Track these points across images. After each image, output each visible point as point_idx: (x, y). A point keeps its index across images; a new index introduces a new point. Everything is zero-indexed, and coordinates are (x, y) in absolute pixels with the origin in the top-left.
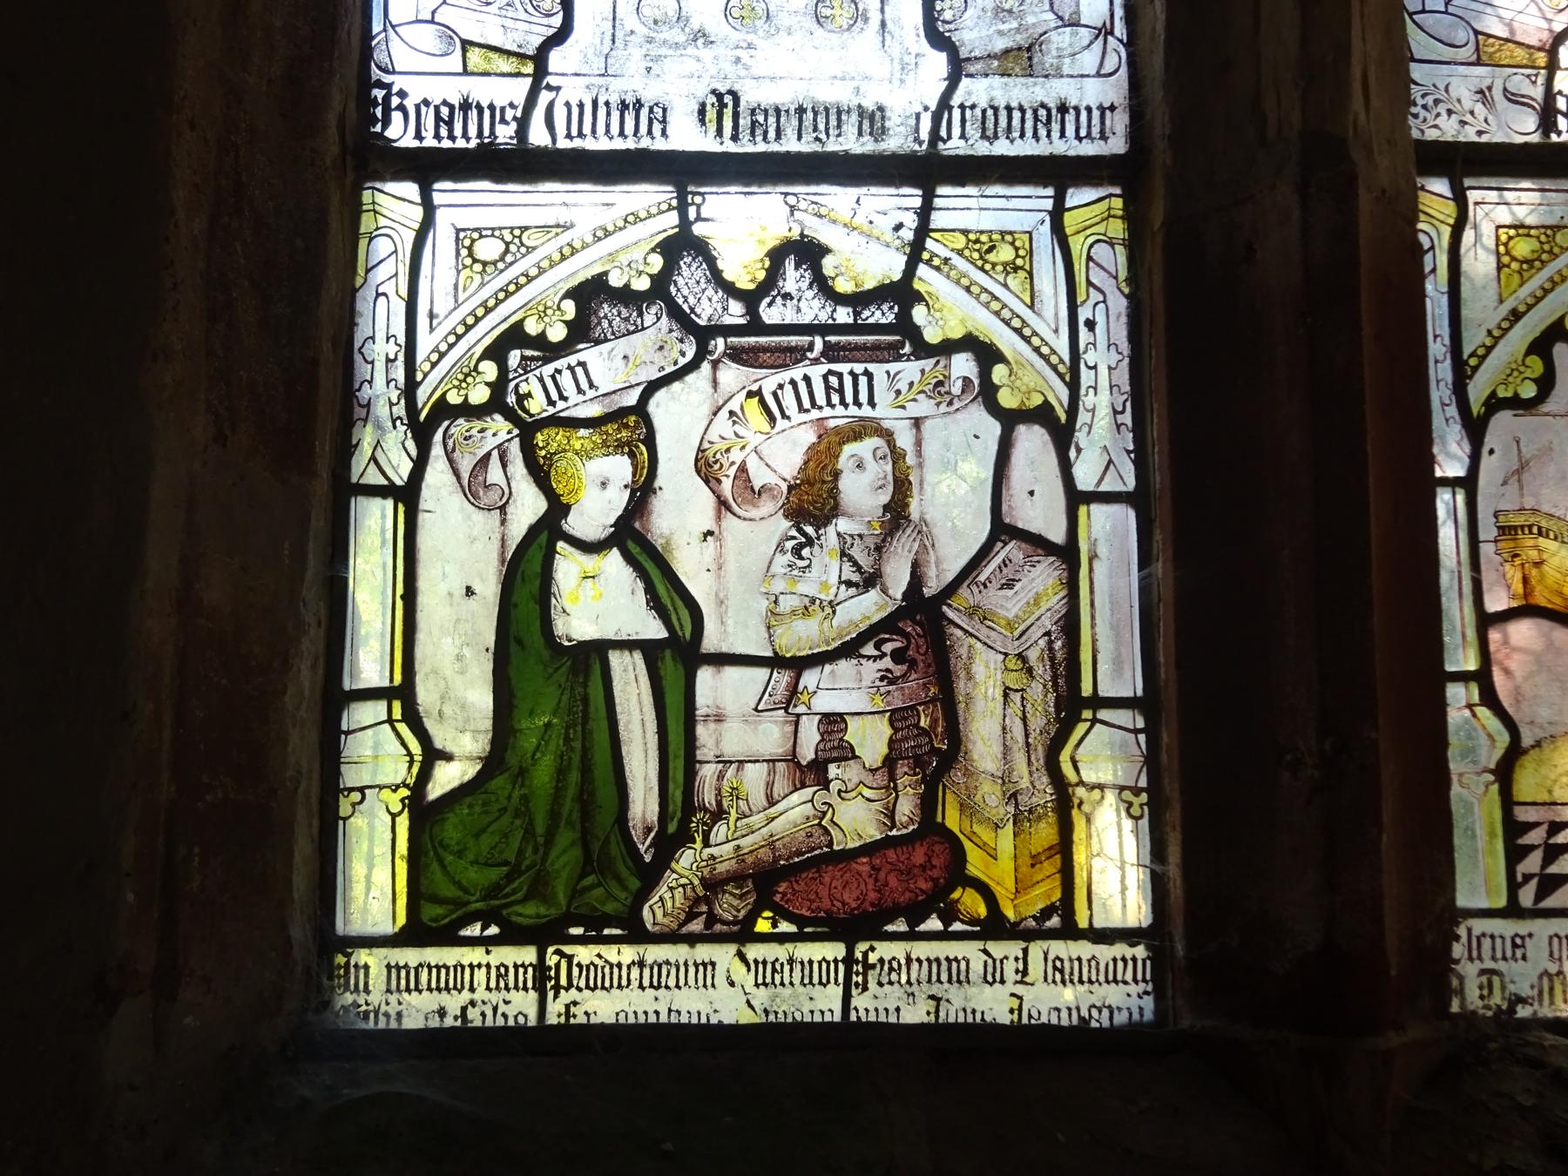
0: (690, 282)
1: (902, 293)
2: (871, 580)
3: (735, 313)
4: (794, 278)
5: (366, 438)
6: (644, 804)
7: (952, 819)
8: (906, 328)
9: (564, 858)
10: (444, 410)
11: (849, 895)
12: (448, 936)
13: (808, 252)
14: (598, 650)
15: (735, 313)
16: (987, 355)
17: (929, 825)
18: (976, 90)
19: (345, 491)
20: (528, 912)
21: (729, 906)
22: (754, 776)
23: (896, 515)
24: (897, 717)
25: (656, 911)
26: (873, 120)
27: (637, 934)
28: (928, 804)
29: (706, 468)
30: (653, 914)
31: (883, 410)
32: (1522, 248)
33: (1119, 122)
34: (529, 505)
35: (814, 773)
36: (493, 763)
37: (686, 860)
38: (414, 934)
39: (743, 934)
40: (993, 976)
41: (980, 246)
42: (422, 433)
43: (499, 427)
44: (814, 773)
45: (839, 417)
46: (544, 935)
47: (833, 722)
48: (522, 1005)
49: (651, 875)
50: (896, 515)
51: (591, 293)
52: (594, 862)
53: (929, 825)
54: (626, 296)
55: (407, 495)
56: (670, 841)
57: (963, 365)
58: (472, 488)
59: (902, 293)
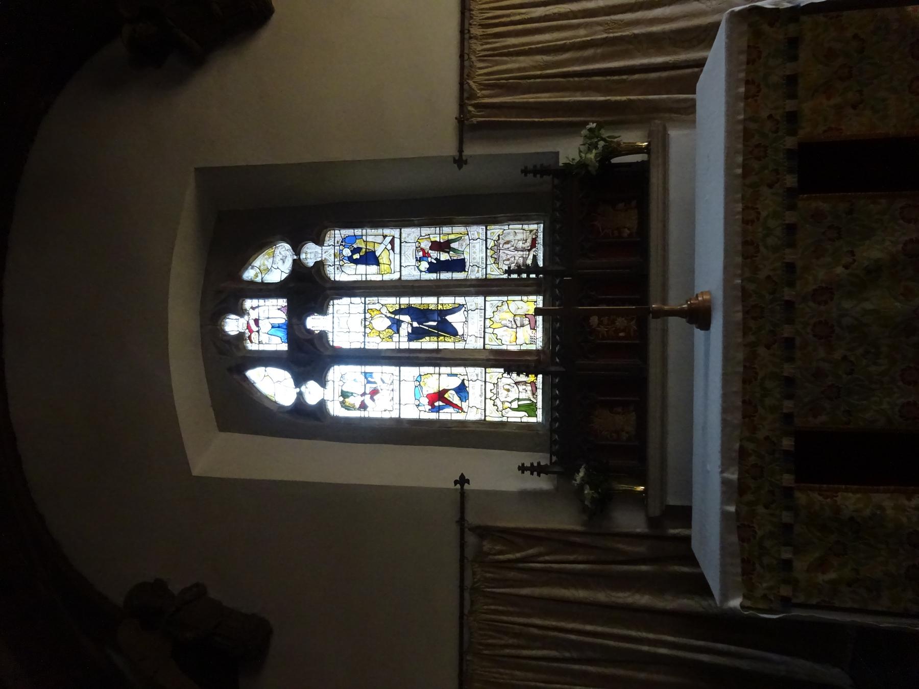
0: (493, 398)
1: (494, 384)
2: (513, 387)
3: (495, 395)
4: (492, 391)
5: (504, 420)
6: (529, 402)
7: (529, 382)
8: (496, 384)
9: (531, 407)
10: (502, 415)
11: (534, 389)
12: (537, 415)
13: (491, 390)
14: (519, 405)
15: (495, 395)
16: (498, 378)
17: (530, 383)
18: (479, 378)
19: (507, 421)
20: (535, 409)
21: (535, 397)
22: (527, 395)
23: (509, 385)
24: (523, 385)
25: (535, 401)
26: (482, 385)
27: (537, 403)
28: (528, 383)
29: (506, 397)
30: (535, 402)
31: (502, 385)
32: (490, 340)
33: (482, 368)
34: (508, 409)
35: (526, 391)
36: (526, 412)
37: (532, 399)
38: (536, 417)
39: (537, 396)
40: (539, 379)
41: (491, 378)
42: (504, 416)
43: (503, 411)
44: (526, 391)
45: (502, 388)
46: (537, 408)
47: (523, 389)
48: (541, 410)
49: (533, 402)
50: (509, 385)
51: (494, 405)
52: (532, 405)
53: (530, 383)
54: (494, 403)
55: (508, 417)
56: (531, 400)
57: (499, 380)
58: (507, 413)
59: (494, 384)
